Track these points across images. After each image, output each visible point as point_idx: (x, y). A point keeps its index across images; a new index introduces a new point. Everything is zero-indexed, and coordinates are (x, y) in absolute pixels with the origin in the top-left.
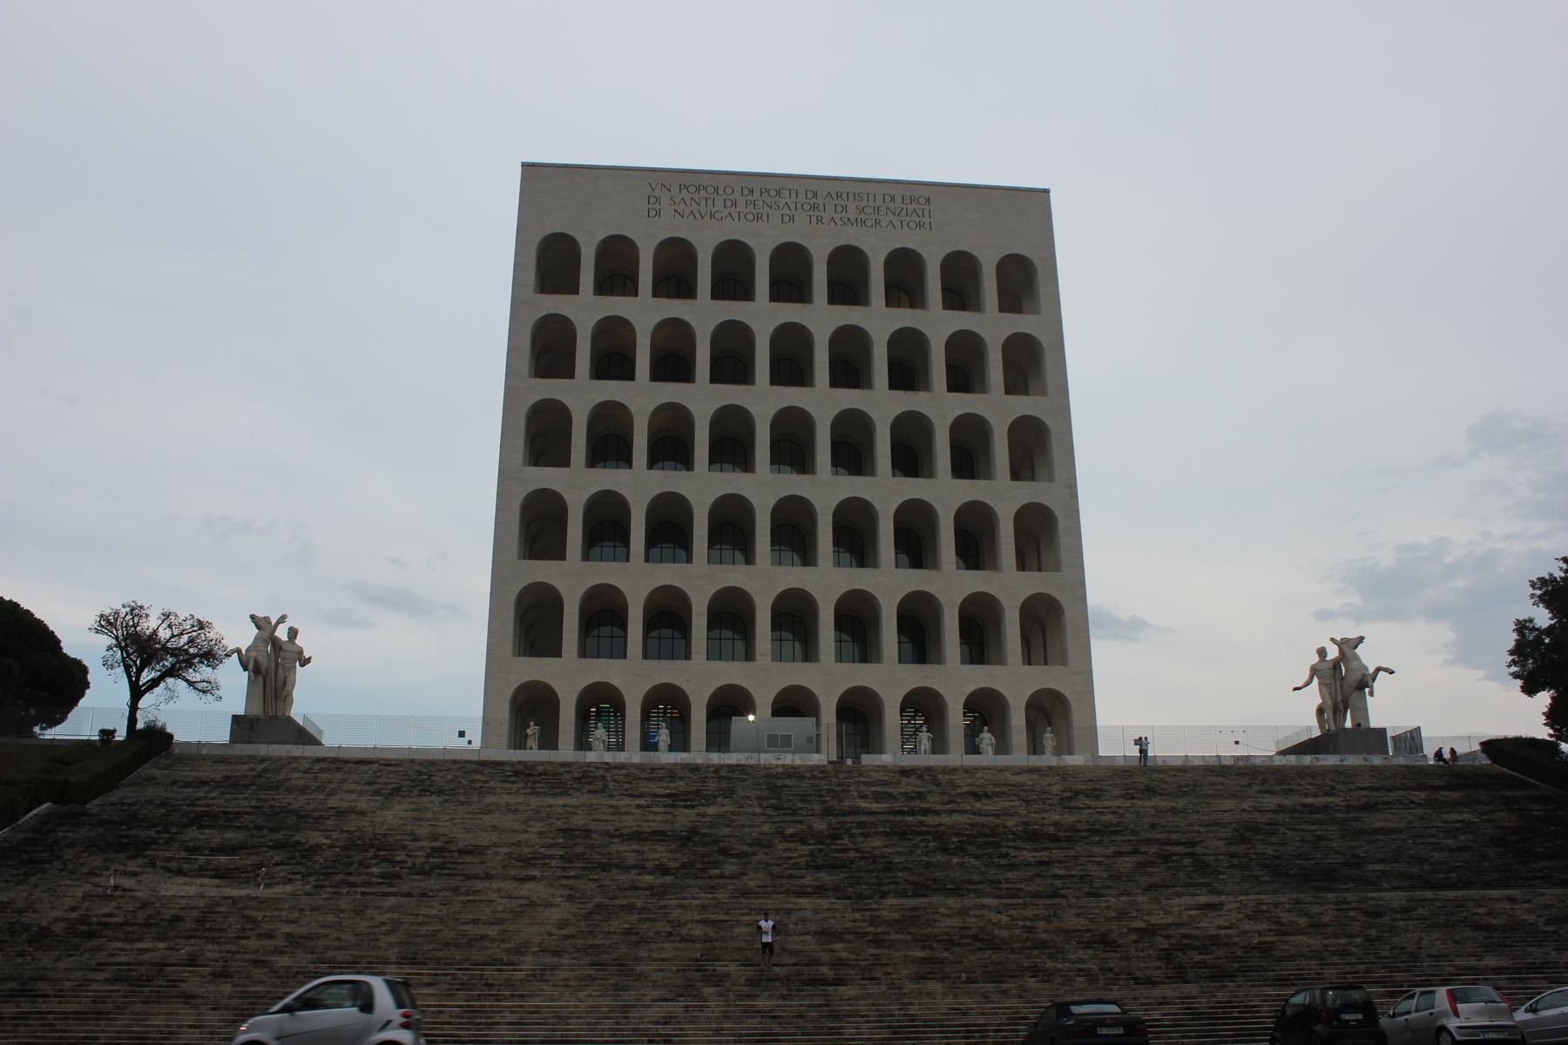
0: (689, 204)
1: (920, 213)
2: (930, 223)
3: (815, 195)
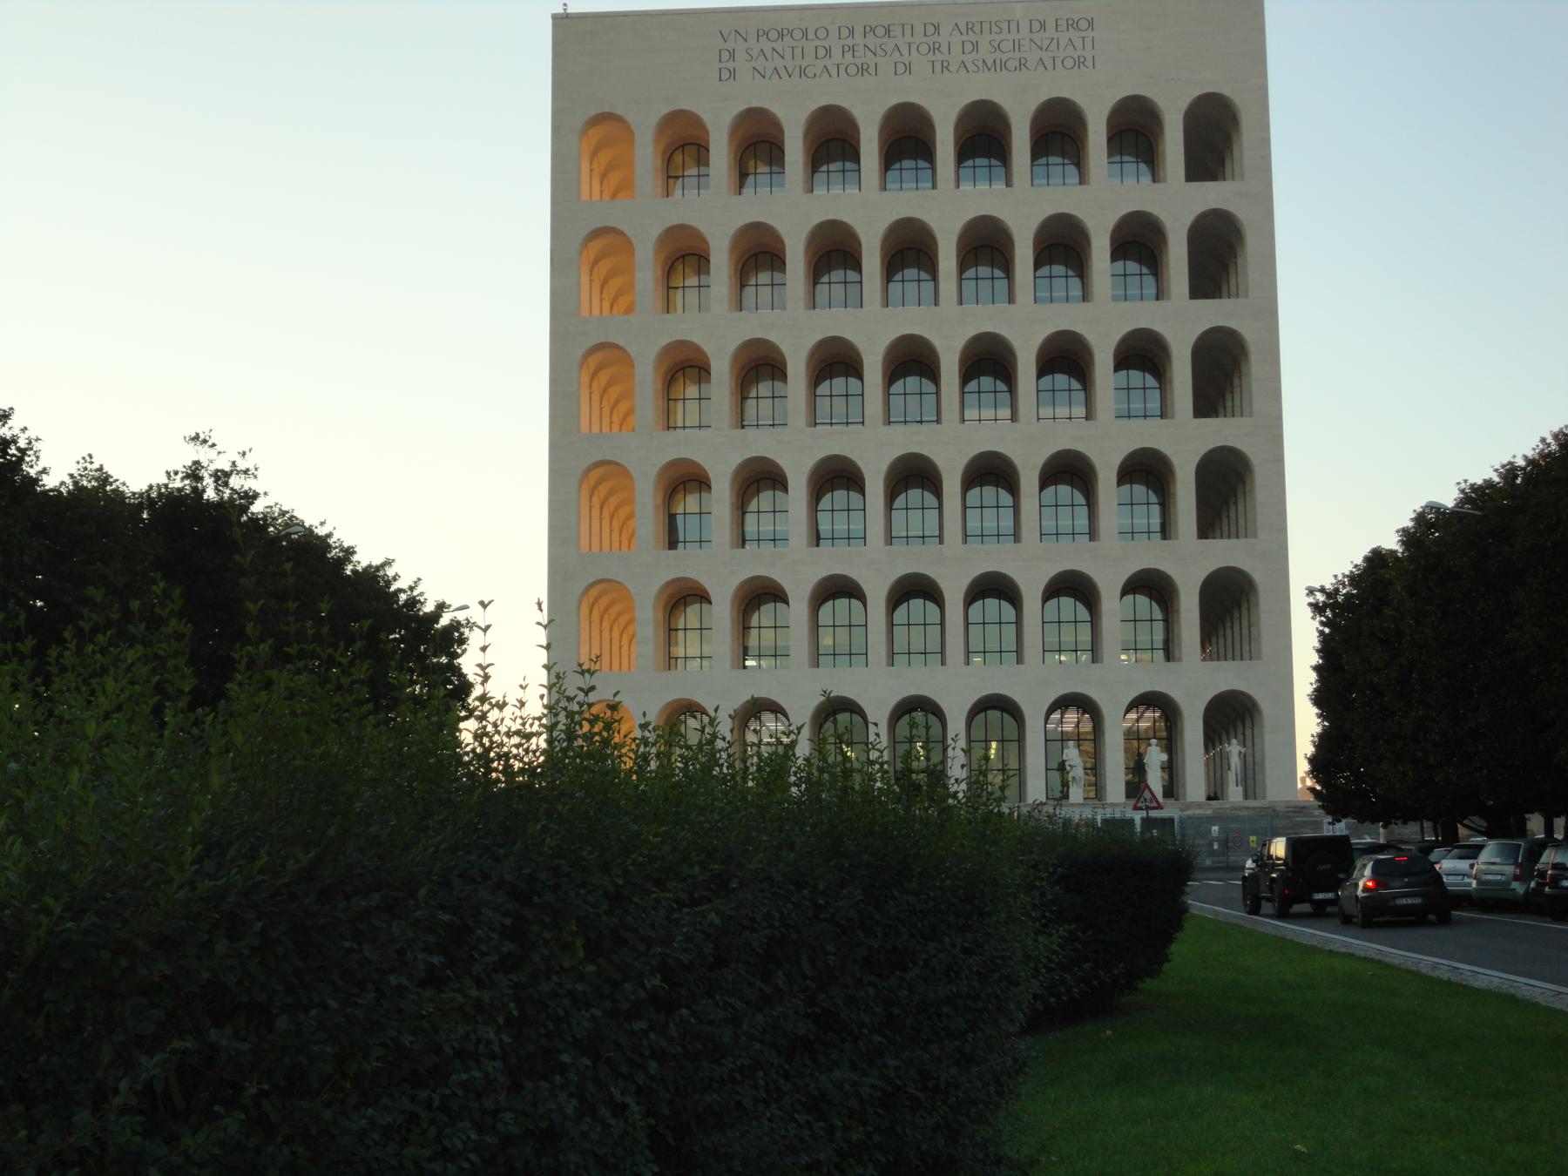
0: (769, 55)
1: (1078, 43)
3: (937, 28)
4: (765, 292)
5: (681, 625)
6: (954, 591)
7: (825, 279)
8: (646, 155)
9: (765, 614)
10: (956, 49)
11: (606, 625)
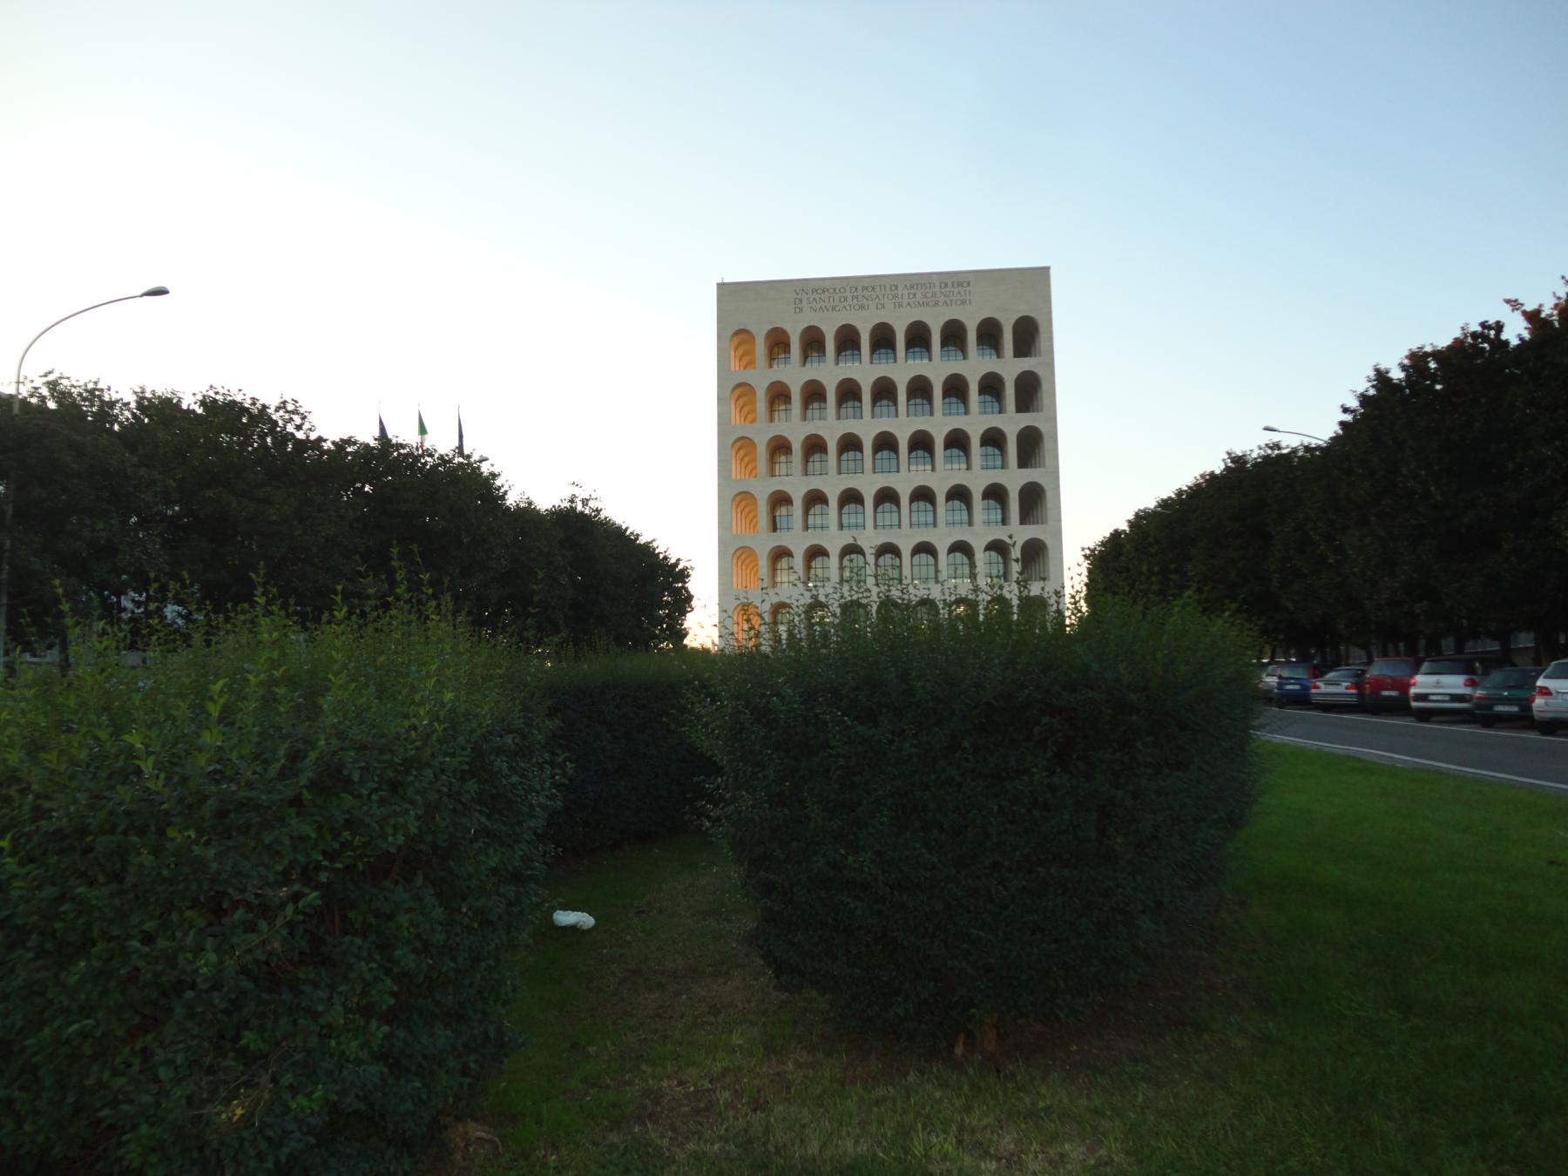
0: (818, 300)
1: (963, 294)
2: (970, 300)
3: (896, 287)
4: (817, 412)
5: (779, 567)
6: (906, 551)
7: (844, 405)
8: (761, 348)
9: (818, 563)
10: (906, 297)
11: (744, 568)
